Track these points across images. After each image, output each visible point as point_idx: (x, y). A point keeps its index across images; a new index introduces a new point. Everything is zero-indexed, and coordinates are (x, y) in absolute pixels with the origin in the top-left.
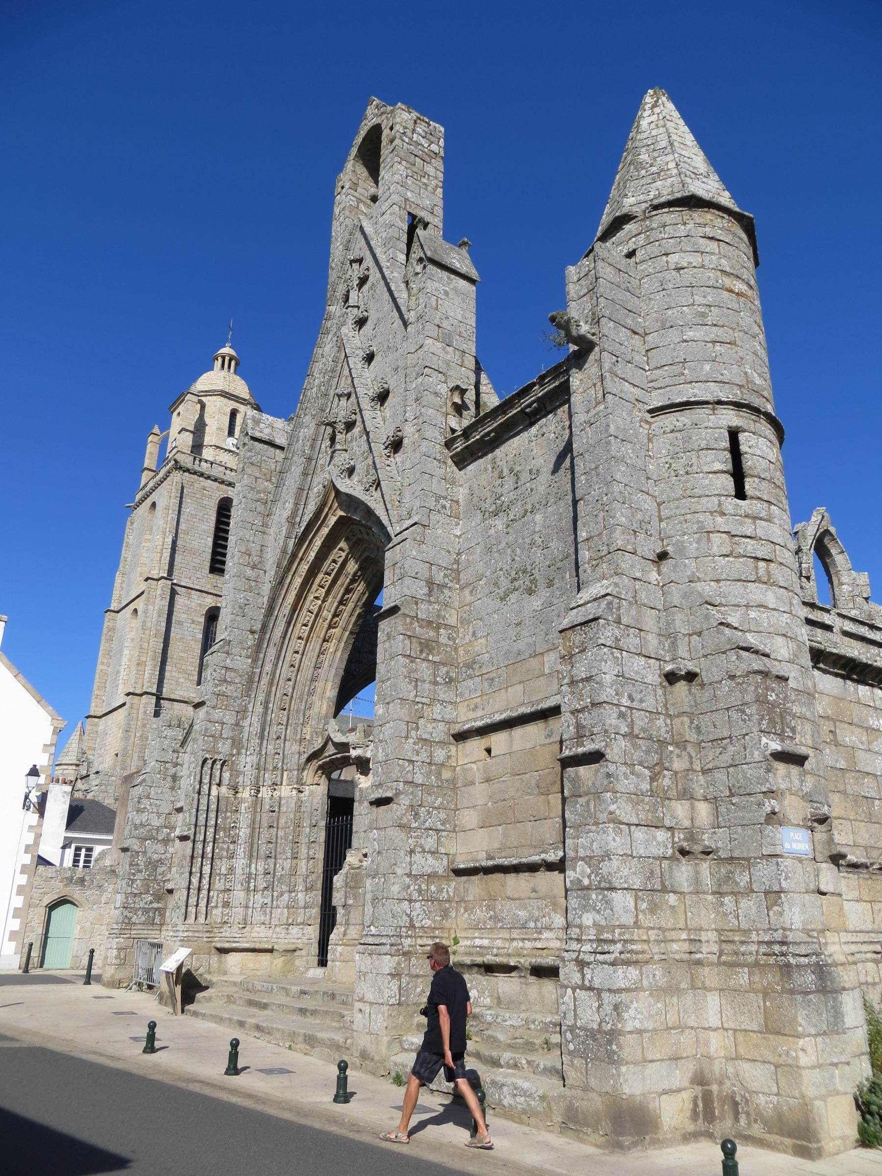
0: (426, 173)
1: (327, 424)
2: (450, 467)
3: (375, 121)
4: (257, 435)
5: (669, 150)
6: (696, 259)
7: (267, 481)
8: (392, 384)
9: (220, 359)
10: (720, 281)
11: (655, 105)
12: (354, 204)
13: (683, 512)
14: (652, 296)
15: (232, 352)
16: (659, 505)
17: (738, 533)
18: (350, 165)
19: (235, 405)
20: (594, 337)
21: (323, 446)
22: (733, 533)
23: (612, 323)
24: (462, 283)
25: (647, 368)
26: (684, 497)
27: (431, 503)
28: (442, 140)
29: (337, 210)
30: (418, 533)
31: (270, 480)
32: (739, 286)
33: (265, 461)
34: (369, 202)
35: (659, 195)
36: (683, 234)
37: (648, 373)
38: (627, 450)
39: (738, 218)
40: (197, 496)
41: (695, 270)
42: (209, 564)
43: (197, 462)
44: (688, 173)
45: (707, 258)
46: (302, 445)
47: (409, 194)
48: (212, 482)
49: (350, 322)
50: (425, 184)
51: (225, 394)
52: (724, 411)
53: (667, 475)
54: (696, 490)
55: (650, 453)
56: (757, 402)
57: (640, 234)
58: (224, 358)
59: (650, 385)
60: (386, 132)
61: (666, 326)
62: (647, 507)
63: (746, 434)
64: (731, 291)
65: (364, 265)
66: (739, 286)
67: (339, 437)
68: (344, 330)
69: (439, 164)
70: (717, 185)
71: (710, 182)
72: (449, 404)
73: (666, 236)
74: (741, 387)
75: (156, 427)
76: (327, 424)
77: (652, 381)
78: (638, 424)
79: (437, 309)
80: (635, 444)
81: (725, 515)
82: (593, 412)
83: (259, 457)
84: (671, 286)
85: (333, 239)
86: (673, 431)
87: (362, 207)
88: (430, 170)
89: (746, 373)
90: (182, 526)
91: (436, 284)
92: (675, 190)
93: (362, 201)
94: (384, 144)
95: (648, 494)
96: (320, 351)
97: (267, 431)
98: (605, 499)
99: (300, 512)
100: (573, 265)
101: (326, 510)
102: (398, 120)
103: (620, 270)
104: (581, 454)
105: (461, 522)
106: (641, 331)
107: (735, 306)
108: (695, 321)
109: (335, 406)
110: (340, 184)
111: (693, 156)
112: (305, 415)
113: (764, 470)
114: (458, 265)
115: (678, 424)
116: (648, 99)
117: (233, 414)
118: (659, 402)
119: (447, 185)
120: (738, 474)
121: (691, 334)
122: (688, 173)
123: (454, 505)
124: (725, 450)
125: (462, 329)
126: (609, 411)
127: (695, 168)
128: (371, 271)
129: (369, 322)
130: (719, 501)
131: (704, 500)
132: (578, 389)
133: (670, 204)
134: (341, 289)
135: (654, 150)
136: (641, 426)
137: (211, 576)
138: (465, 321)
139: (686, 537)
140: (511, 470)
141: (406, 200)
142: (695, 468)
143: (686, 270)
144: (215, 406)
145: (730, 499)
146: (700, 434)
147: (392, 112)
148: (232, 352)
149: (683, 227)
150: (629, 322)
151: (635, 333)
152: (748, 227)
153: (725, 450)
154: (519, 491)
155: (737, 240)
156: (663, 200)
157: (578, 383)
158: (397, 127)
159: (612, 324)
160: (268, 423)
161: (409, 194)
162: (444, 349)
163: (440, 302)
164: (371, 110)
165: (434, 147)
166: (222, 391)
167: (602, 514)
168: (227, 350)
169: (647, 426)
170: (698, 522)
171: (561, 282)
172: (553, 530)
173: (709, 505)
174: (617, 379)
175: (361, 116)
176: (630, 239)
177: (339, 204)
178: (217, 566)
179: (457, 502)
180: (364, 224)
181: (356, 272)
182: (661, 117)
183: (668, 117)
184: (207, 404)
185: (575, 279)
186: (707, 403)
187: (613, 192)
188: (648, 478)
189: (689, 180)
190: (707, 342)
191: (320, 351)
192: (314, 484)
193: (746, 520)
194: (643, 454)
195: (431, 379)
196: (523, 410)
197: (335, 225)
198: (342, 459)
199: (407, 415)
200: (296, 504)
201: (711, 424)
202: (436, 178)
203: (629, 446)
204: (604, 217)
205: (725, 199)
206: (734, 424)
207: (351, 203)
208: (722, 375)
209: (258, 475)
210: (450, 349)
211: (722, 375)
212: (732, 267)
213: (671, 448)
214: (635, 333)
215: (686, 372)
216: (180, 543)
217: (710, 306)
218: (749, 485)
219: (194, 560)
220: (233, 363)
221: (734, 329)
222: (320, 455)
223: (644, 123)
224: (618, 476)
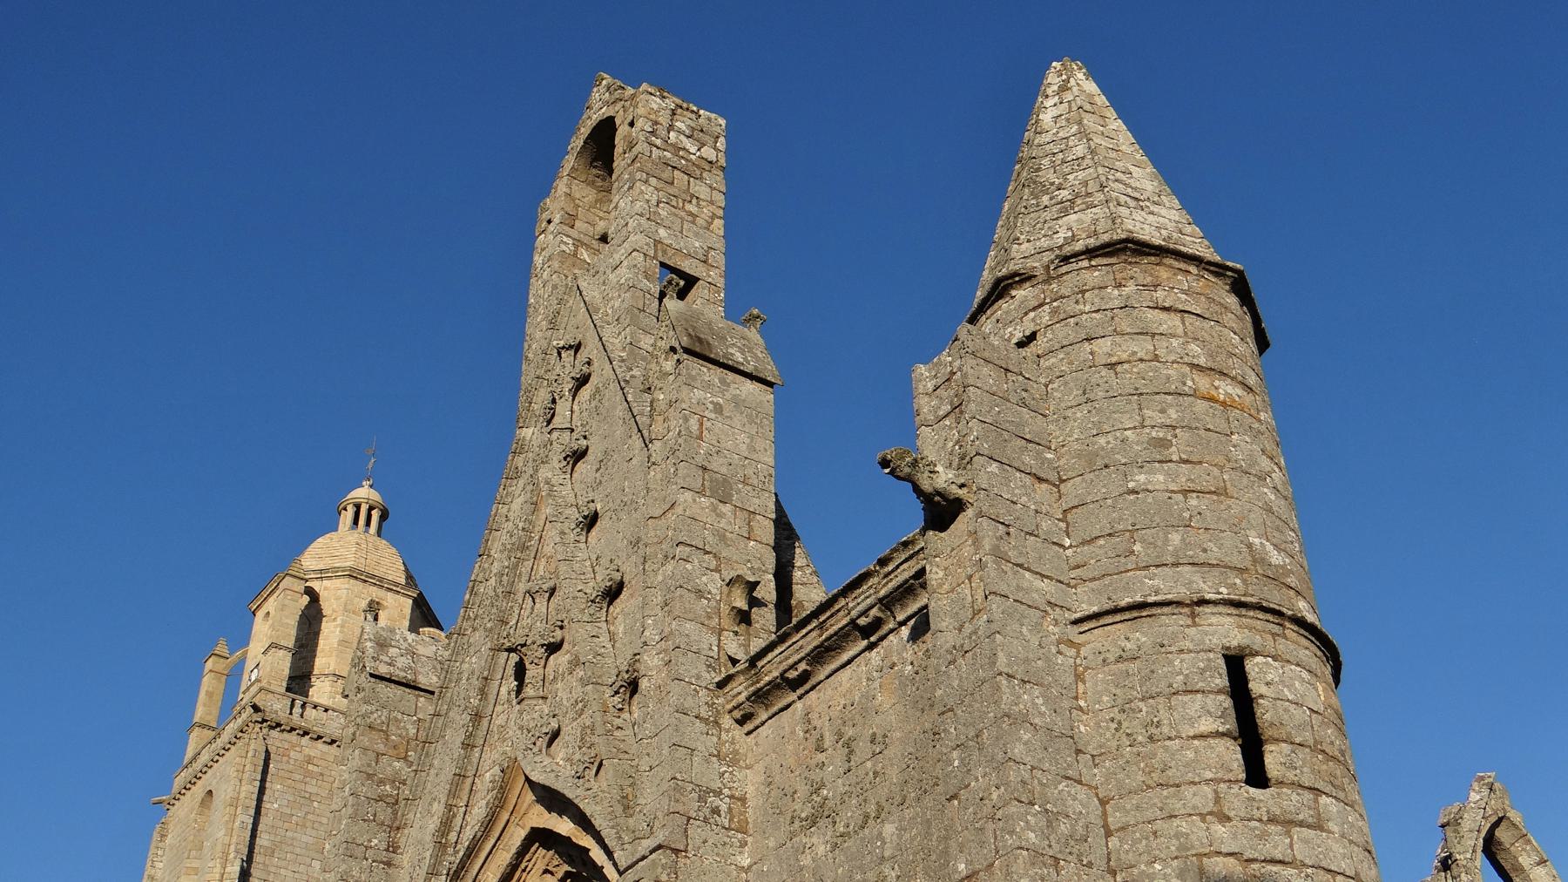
0: (692, 196)
1: (510, 650)
2: (728, 731)
3: (605, 112)
4: (383, 670)
5: (1088, 161)
6: (1142, 347)
7: (399, 759)
8: (629, 570)
9: (351, 510)
10: (1190, 383)
11: (1064, 88)
12: (569, 249)
13: (1149, 815)
14: (1069, 413)
15: (375, 496)
16: (1103, 802)
17: (1256, 855)
18: (561, 186)
19: (375, 593)
20: (965, 490)
21: (504, 690)
22: (1248, 854)
23: (995, 465)
24: (750, 387)
25: (1067, 542)
26: (1149, 787)
27: (692, 806)
28: (722, 139)
29: (538, 260)
30: (663, 867)
31: (405, 758)
32: (1226, 389)
33: (397, 720)
34: (595, 244)
35: (1074, 238)
36: (1117, 303)
37: (1069, 552)
38: (1032, 698)
39: (1219, 270)
40: (298, 777)
41: (1142, 366)
43: (298, 710)
44: (1123, 199)
45: (1162, 343)
46: (465, 691)
47: (662, 232)
48: (326, 748)
49: (556, 461)
50: (691, 214)
51: (354, 575)
52: (1214, 620)
53: (1114, 744)
54: (1169, 773)
55: (1082, 703)
56: (1274, 598)
57: (1041, 305)
58: (358, 507)
59: (1073, 574)
60: (622, 131)
61: (1096, 463)
62: (1079, 808)
63: (1259, 659)
64: (1212, 399)
65: (583, 355)
66: (1226, 389)
67: (532, 672)
68: (544, 473)
69: (717, 179)
70: (1175, 215)
71: (1163, 212)
72: (725, 610)
73: (1087, 309)
74: (1242, 571)
75: (222, 641)
76: (510, 650)
77: (1078, 567)
78: (1054, 649)
79: (700, 438)
80: (1049, 686)
81: (1229, 819)
82: (968, 628)
83: (385, 712)
84: (1101, 394)
85: (531, 310)
86: (1120, 659)
87: (584, 254)
88: (700, 189)
89: (1250, 546)
90: (263, 840)
91: (698, 394)
92: (1100, 229)
93: (583, 244)
94: (618, 150)
95: (1080, 782)
96: (503, 510)
97: (402, 662)
98: (994, 796)
99: (458, 821)
100: (925, 363)
101: (505, 816)
102: (641, 111)
103: (1007, 370)
104: (951, 710)
105: (750, 840)
106: (1053, 477)
107: (1223, 426)
108: (1145, 455)
109: (525, 613)
110: (545, 216)
111: (1132, 169)
112: (474, 630)
113: (1300, 727)
114: (739, 357)
115: (1129, 646)
116: (1053, 80)
118: (1091, 604)
119: (729, 215)
120: (1250, 739)
121: (1142, 478)
122: (1123, 199)
123: (737, 806)
124: (1220, 692)
125: (749, 472)
126: (994, 627)
127: (1135, 189)
128: (596, 364)
129: (590, 457)
130: (1216, 792)
131: (1188, 792)
132: (941, 585)
133: (1090, 253)
134: (542, 397)
135: (1064, 162)
136: (1059, 652)
138: (755, 456)
139: (1158, 866)
140: (840, 735)
141: (657, 242)
142: (1166, 730)
143: (1126, 366)
144: (338, 599)
145: (1235, 788)
146: (1171, 663)
147: (633, 97)
148: (375, 496)
149: (1116, 292)
150: (1028, 460)
151: (1040, 480)
152: (1241, 288)
153: (1220, 692)
154: (852, 777)
155: (1217, 308)
156: (1079, 246)
157: (941, 574)
158: (639, 124)
159: (994, 467)
160: (405, 645)
161: (662, 232)
162: (714, 509)
163: (707, 424)
164: (598, 95)
165: (708, 153)
166: (352, 569)
167: (990, 826)
169: (1073, 652)
170: (1178, 835)
171: (907, 393)
172: (915, 854)
173: (1197, 801)
174: (1008, 567)
175: (582, 103)
176: (1026, 314)
177: (543, 250)
179: (743, 800)
180: (583, 284)
181: (568, 367)
182: (1075, 108)
183: (1088, 107)
184: (323, 595)
185: (930, 386)
186: (1179, 603)
187: (1000, 232)
188: (1078, 752)
189: (1124, 211)
190: (1173, 492)
191: (503, 510)
192: (485, 765)
193: (1272, 828)
194: (1066, 704)
195: (689, 566)
196: (853, 621)
197: (535, 285)
198: (537, 714)
199: (647, 633)
200: (449, 807)
201: (1188, 645)
202: (712, 202)
203: (1037, 691)
204: (985, 273)
205: (1195, 243)
206: (1235, 643)
207: (563, 247)
208: (1205, 551)
209: (381, 748)
210: (726, 509)
211: (1205, 551)
212: (1211, 355)
213: (1118, 691)
214: (1040, 480)
215: (1137, 547)
217: (1174, 428)
218: (1273, 759)
220: (375, 514)
221: (1221, 468)
222: (499, 708)
223: (1046, 118)
224: (1018, 750)
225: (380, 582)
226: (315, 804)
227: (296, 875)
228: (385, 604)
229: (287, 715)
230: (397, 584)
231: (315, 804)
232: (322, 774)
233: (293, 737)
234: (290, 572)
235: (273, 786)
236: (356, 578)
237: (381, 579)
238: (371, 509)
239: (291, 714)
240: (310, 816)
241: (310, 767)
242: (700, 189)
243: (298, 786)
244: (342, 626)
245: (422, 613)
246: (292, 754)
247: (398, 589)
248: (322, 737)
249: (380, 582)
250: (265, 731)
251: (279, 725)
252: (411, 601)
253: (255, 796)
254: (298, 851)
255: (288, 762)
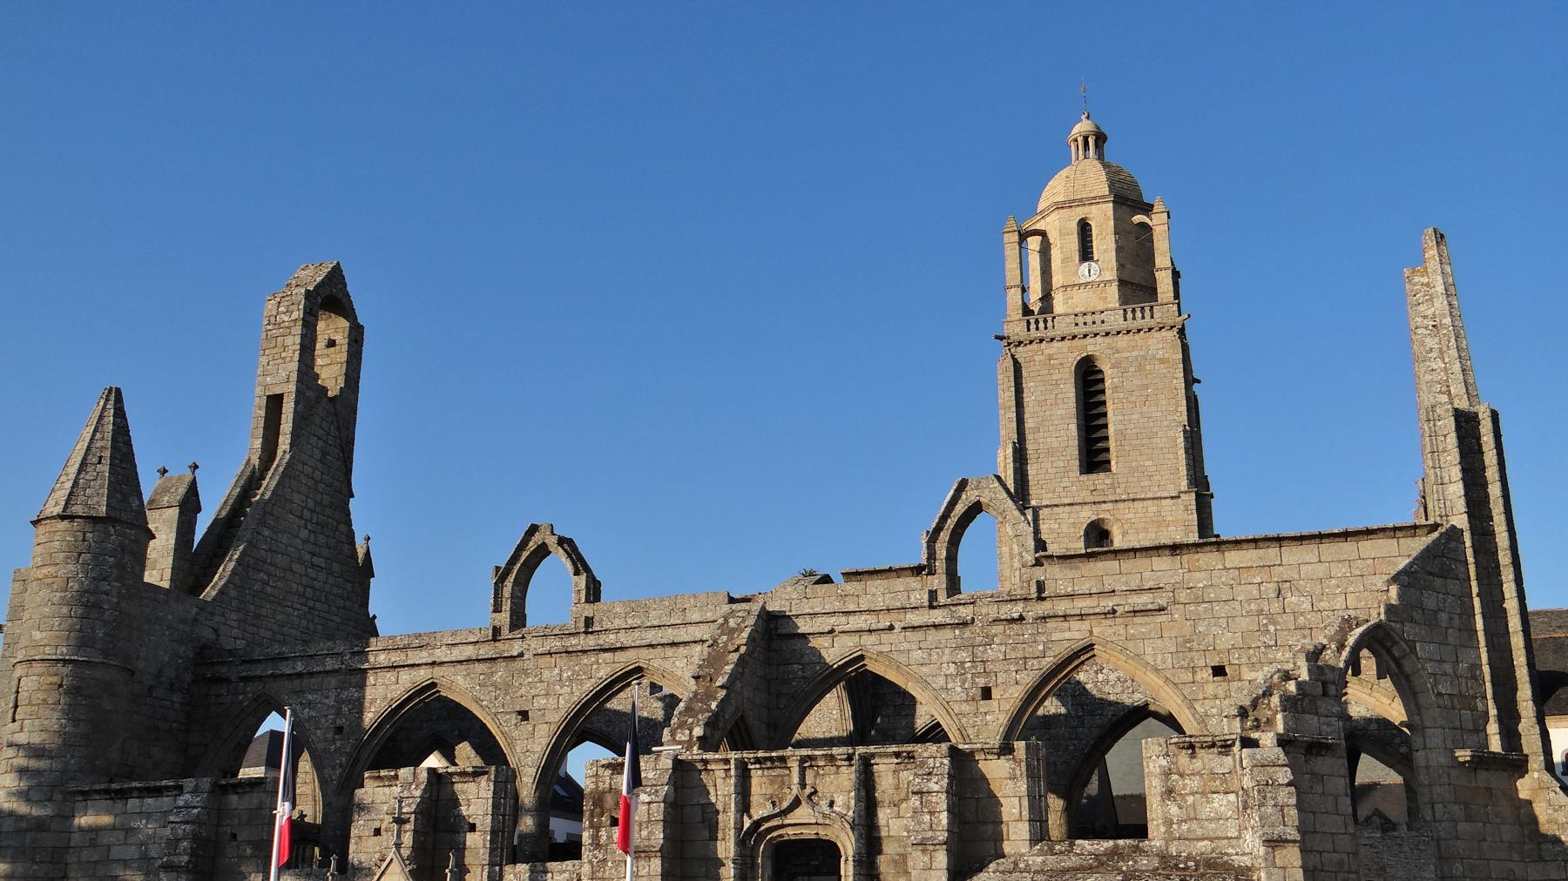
19: (1080, 212)
40: (1044, 372)
42: (1077, 463)
43: (1033, 326)
90: (1029, 423)
117: (1084, 228)
137: (1084, 477)
168: (1083, 127)
178: (1093, 457)
216: (1030, 446)
219: (1054, 465)
220: (1091, 141)
225: (1082, 202)
226: (1062, 386)
227: (1059, 439)
228: (1091, 216)
229: (1026, 333)
230: (1095, 198)
231: (1062, 386)
232: (1061, 364)
233: (1034, 346)
234: (1006, 230)
235: (1028, 385)
236: (1063, 208)
237: (1081, 200)
238: (1086, 139)
239: (1029, 330)
240: (1059, 396)
241: (1052, 362)
242: (289, 340)
243: (1046, 378)
244: (1061, 248)
245: (1129, 206)
246: (1036, 358)
247: (1097, 201)
248: (1054, 339)
249: (1082, 202)
250: (1012, 350)
251: (1020, 343)
252: (1111, 205)
253: (1013, 398)
254: (1056, 422)
255: (1035, 365)
